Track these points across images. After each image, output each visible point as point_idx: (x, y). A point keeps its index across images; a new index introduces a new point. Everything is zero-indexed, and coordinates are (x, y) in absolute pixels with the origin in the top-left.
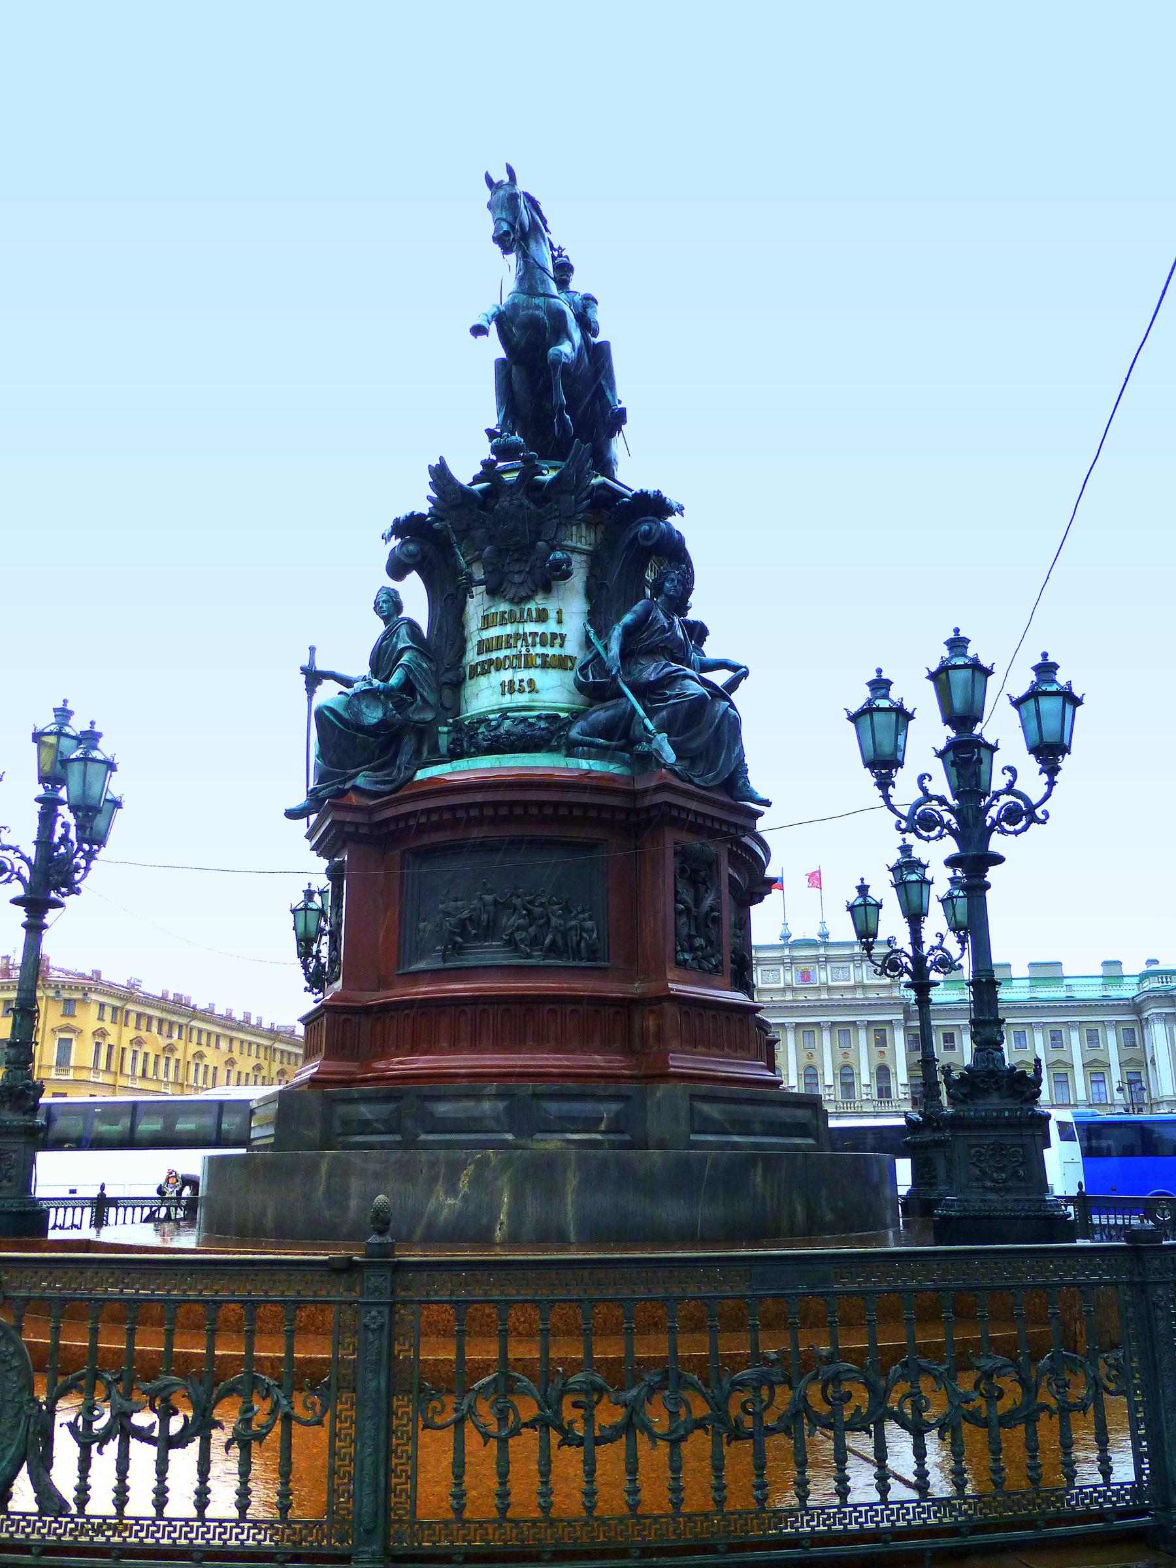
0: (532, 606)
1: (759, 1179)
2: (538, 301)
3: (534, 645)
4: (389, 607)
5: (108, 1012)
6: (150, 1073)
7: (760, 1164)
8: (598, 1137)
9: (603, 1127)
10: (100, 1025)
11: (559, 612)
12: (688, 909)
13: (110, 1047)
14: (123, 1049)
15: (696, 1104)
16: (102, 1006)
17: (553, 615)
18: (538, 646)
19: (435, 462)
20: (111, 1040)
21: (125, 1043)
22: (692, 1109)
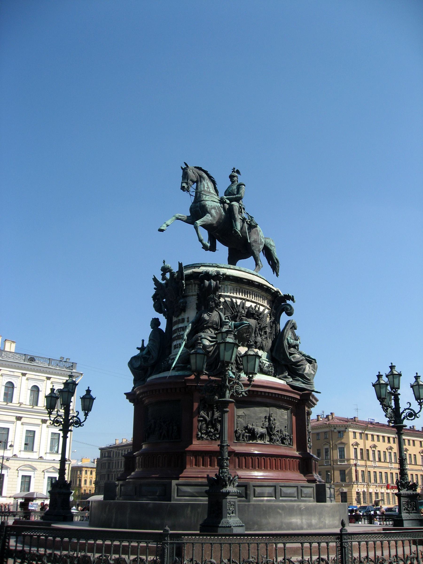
0: (180, 318)
1: (189, 511)
2: (198, 204)
3: (181, 331)
4: (155, 323)
5: (358, 435)
6: (382, 460)
7: (190, 506)
8: (156, 497)
9: (158, 494)
10: (355, 440)
11: (188, 318)
12: (205, 419)
13: (361, 449)
14: (368, 450)
15: (179, 487)
16: (354, 433)
17: (186, 320)
18: (182, 331)
19: (153, 277)
20: (361, 446)
21: (368, 447)
22: (178, 489)
